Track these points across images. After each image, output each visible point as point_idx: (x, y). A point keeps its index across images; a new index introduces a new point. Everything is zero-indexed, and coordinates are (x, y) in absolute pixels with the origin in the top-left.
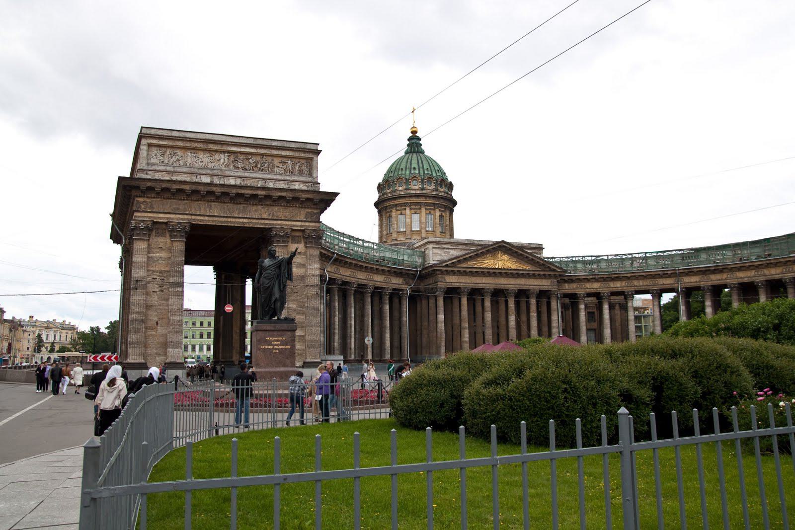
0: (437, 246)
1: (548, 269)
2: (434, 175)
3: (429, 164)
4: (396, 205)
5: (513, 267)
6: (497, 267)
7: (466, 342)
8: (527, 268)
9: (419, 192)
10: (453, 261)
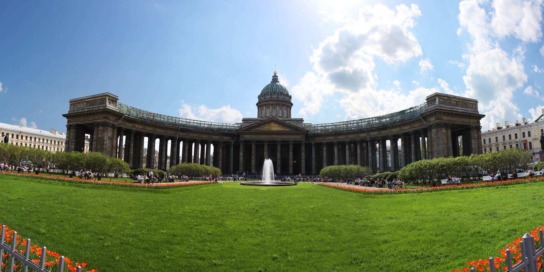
0: (246, 122)
1: (299, 130)
2: (278, 91)
3: (276, 86)
4: (261, 106)
5: (280, 130)
6: (271, 130)
7: (253, 165)
8: (288, 130)
9: (269, 99)
10: (246, 128)
